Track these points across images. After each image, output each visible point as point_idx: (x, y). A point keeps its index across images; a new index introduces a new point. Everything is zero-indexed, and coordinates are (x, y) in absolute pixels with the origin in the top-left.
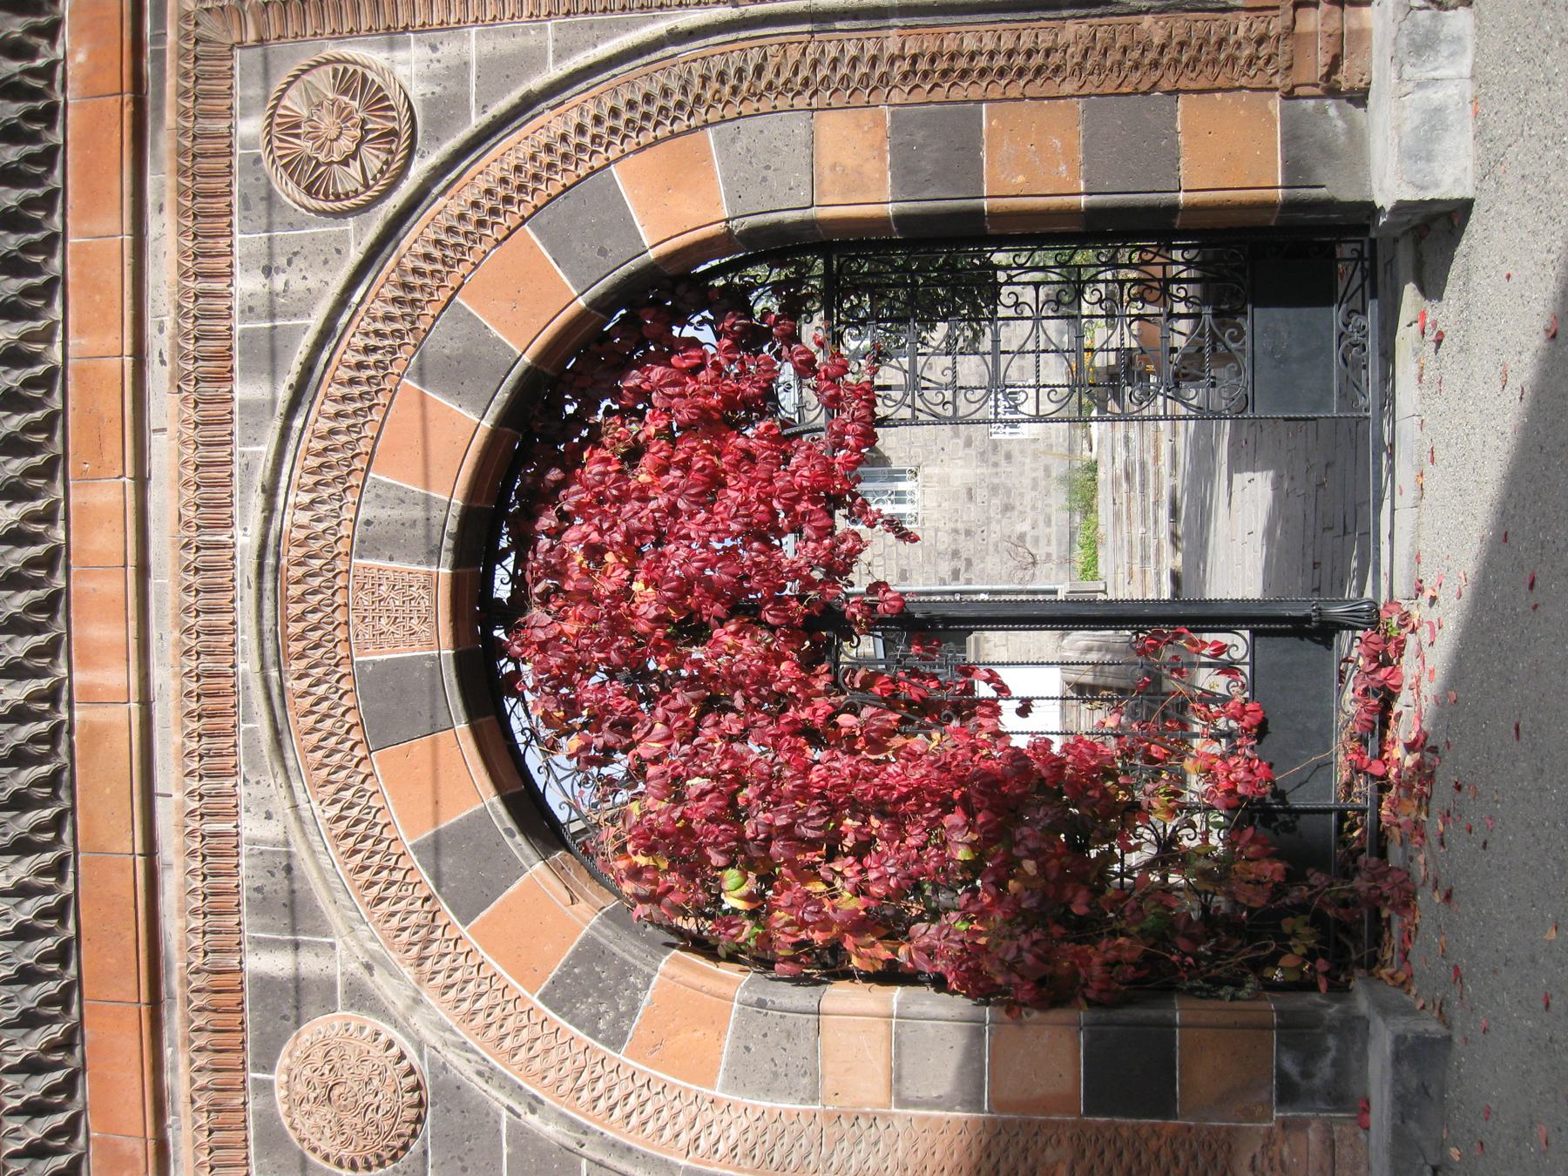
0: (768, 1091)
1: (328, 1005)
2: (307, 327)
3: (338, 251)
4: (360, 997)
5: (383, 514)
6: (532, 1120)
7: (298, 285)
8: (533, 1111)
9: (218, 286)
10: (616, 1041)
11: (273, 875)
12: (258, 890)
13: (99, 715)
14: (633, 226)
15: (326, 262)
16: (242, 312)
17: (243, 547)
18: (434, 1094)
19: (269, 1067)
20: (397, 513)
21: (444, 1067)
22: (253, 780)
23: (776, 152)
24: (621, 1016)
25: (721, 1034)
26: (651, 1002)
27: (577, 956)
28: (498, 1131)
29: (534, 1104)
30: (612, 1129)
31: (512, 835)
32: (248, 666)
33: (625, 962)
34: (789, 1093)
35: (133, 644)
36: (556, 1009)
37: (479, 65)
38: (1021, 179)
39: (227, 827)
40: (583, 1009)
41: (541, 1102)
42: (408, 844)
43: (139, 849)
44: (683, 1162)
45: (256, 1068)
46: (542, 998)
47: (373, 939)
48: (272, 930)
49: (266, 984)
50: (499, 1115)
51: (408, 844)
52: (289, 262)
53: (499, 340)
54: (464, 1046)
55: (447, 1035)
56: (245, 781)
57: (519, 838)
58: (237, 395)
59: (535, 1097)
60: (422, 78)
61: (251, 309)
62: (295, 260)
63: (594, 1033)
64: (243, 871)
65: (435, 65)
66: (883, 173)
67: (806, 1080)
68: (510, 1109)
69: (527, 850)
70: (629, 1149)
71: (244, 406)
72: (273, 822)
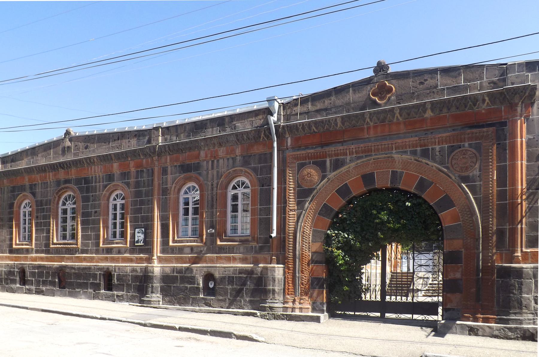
2: (429, 159)
5: (398, 174)
7: (437, 157)
9: (437, 143)
12: (339, 160)
13: (366, 130)
16: (433, 148)
17: (392, 153)
18: (310, 189)
22: (356, 157)
43: (345, 140)
47: (332, 178)
49: (325, 162)
52: (441, 155)
54: (317, 193)
61: (433, 149)
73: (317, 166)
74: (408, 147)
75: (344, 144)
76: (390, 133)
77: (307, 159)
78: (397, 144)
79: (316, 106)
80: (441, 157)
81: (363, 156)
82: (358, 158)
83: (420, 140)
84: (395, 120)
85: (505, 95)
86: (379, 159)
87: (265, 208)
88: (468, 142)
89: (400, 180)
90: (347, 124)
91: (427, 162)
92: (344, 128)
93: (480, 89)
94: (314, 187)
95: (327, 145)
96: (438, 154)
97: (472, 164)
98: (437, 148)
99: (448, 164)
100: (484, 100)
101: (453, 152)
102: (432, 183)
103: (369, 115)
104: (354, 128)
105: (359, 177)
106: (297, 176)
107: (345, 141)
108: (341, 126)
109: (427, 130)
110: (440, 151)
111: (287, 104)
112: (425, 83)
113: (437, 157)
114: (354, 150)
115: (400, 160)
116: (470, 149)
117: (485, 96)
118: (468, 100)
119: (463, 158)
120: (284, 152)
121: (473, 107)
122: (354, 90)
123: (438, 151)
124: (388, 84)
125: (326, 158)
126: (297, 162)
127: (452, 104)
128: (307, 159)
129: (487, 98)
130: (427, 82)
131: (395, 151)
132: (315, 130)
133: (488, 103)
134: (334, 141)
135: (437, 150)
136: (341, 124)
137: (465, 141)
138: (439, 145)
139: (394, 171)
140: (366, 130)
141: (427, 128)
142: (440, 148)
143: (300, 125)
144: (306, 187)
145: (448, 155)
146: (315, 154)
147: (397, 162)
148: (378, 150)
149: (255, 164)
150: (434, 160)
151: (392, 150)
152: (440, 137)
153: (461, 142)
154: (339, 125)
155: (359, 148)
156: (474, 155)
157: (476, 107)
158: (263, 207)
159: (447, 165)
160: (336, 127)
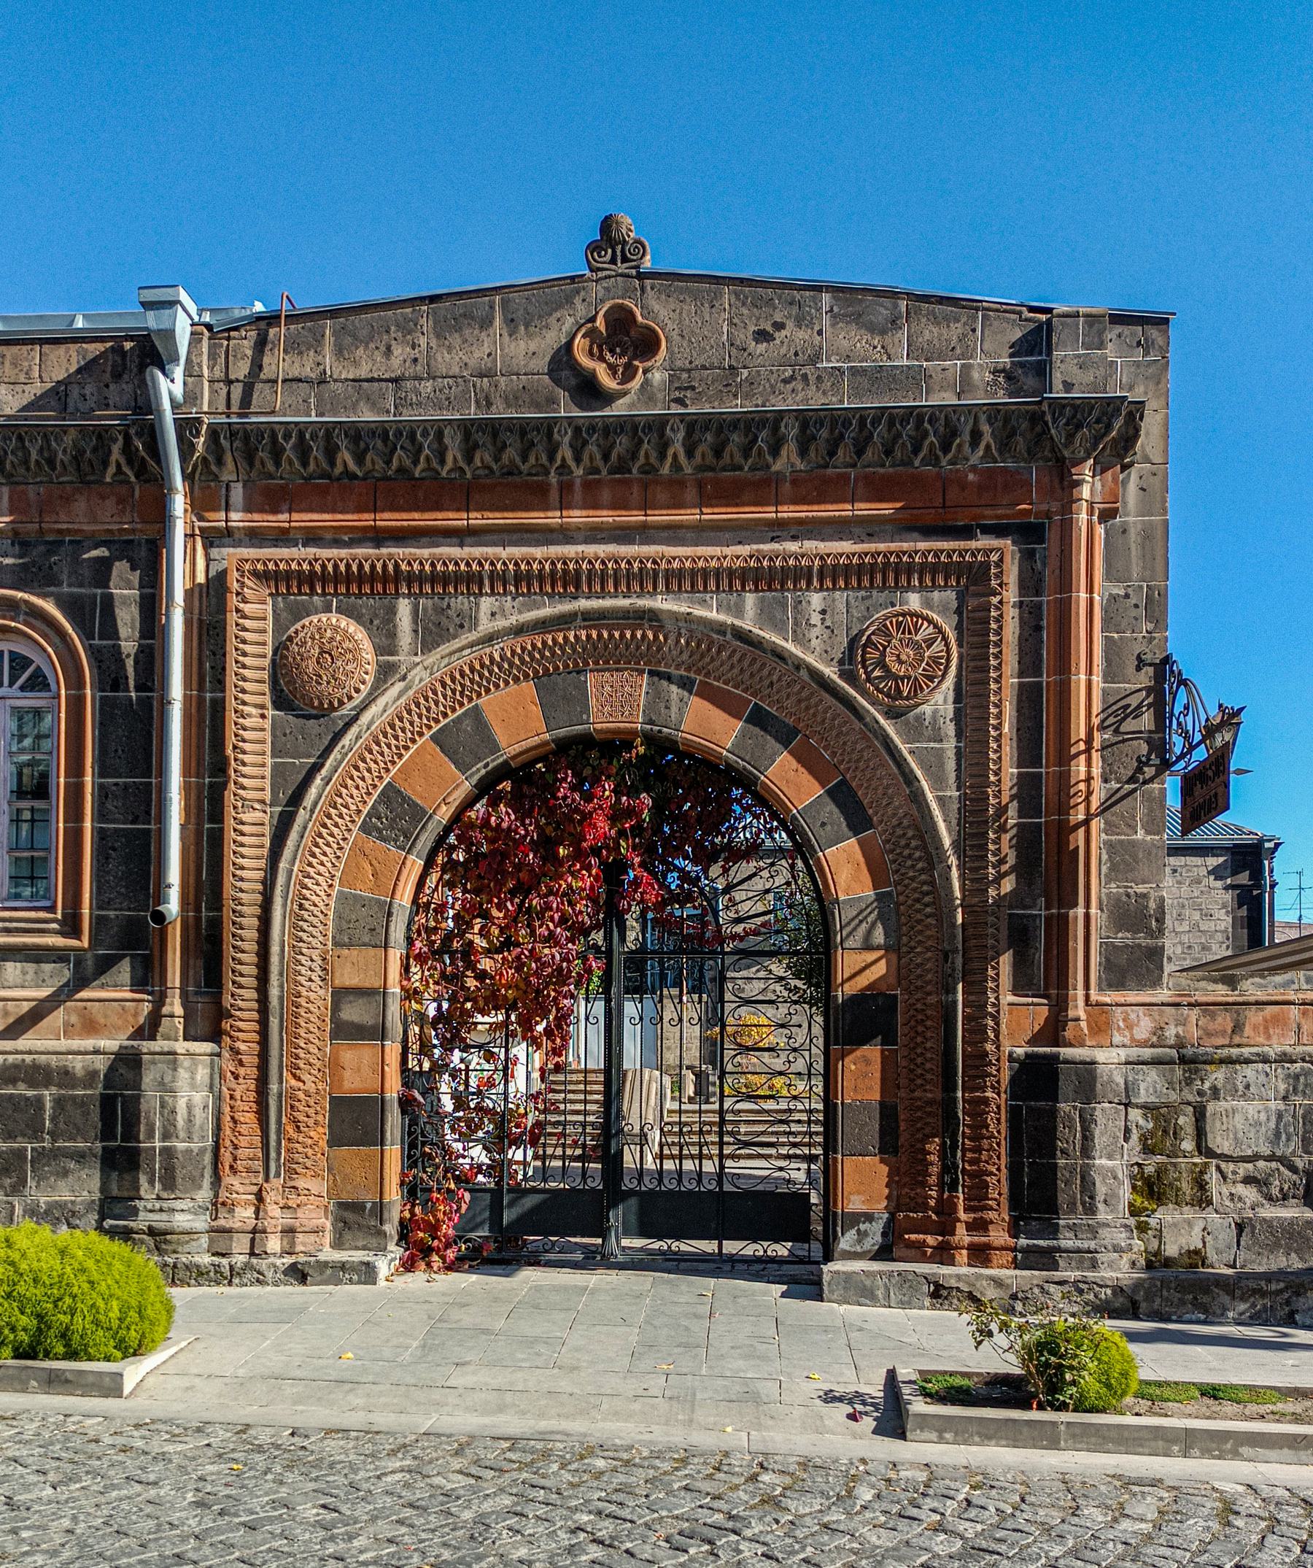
1: (379, 650)
7: (815, 632)
10: (365, 828)
15: (826, 652)
24: (379, 831)
32: (584, 604)
36: (383, 793)
40: (382, 809)
47: (421, 680)
52: (827, 627)
62: (828, 631)
75: (468, 540)
79: (356, 363)
84: (665, 470)
85: (1046, 423)
86: (604, 618)
87: (126, 786)
92: (469, 476)
93: (962, 391)
96: (815, 619)
100: (976, 436)
102: (797, 732)
104: (510, 478)
108: (461, 464)
110: (823, 612)
112: (777, 335)
117: (983, 418)
118: (926, 425)
121: (940, 453)
122: (512, 320)
124: (640, 319)
127: (871, 434)
129: (986, 428)
130: (784, 333)
132: (352, 466)
136: (459, 457)
149: (81, 585)
157: (950, 456)
158: (116, 784)
160: (435, 464)
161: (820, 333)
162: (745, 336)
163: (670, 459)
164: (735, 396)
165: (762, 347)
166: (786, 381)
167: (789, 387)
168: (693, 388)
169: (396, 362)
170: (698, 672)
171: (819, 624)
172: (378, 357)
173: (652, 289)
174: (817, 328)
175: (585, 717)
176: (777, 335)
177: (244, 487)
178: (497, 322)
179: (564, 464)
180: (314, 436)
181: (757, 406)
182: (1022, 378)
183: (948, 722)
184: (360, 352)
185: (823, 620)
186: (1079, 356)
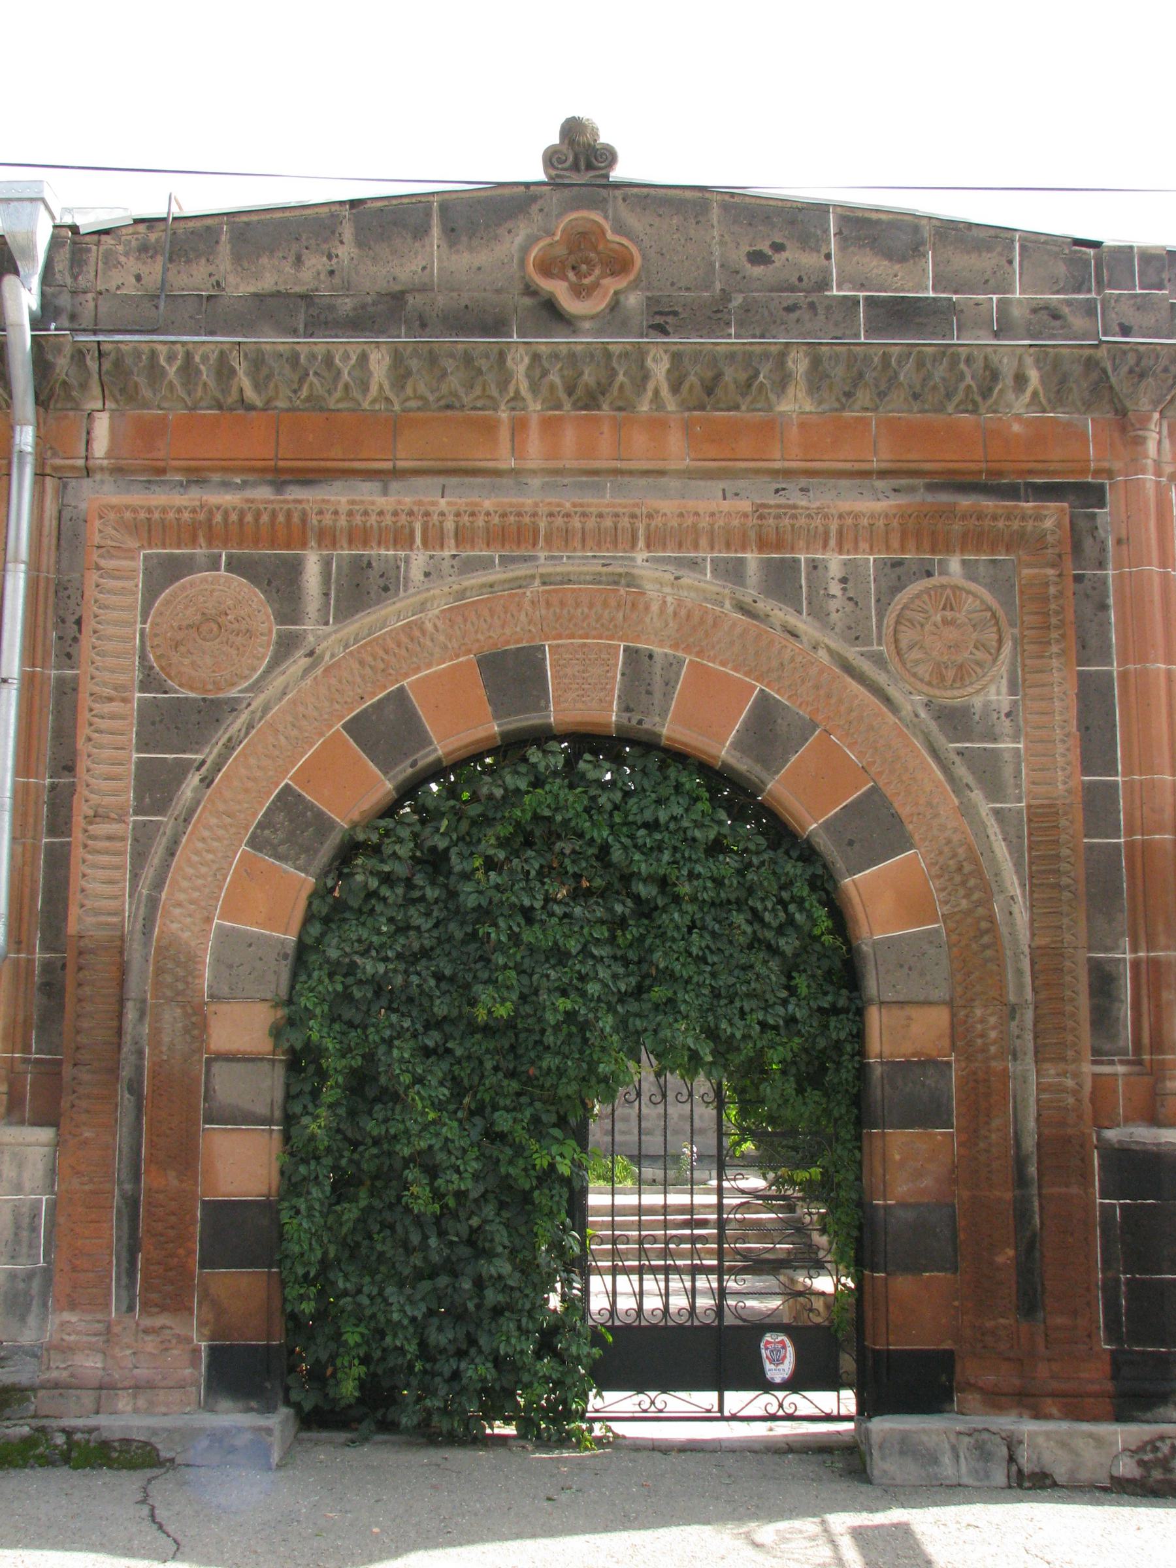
0: (218, 960)
1: (282, 618)
2: (800, 612)
3: (857, 638)
4: (287, 645)
5: (657, 669)
6: (194, 779)
7: (833, 605)
8: (202, 780)
9: (832, 542)
11: (382, 576)
12: (369, 565)
13: (504, 434)
14: (869, 867)
15: (850, 628)
16: (813, 560)
17: (633, 559)
18: (212, 701)
19: (230, 567)
20: (657, 679)
21: (233, 710)
22: (454, 562)
23: (922, 974)
24: (274, 848)
25: (258, 924)
26: (285, 871)
27: (320, 815)
28: (184, 752)
29: (207, 782)
30: (188, 841)
31: (412, 766)
33: (316, 852)
34: (216, 976)
35: (559, 464)
36: (279, 796)
37: (993, 750)
38: (897, 1157)
39: (418, 541)
40: (280, 817)
41: (208, 786)
42: (405, 683)
43: (401, 464)
44: (164, 895)
45: (230, 557)
46: (287, 785)
47: (333, 656)
48: (339, 574)
49: (295, 568)
50: (197, 752)
51: (405, 683)
52: (850, 599)
53: (787, 761)
54: (250, 726)
55: (259, 714)
56: (454, 556)
57: (410, 771)
58: (748, 555)
59: (212, 781)
60: (986, 705)
61: (815, 568)
62: (851, 604)
63: (260, 825)
64: (383, 552)
65: (995, 716)
66: (904, 1056)
67: (226, 989)
68: (203, 762)
69: (401, 777)
70: (173, 855)
71: (741, 561)
72: (422, 578)
73: (254, 579)
74: (703, 542)
75: (395, 485)
76: (619, 465)
77: (202, 540)
78: (658, 521)
80: (850, 607)
81: (492, 559)
82: (469, 566)
83: (761, 517)
84: (644, 407)
85: (1104, 371)
86: (569, 581)
88: (962, 552)
89: (668, 696)
90: (415, 390)
91: (792, 620)
92: (397, 407)
93: (1000, 330)
94: (233, 693)
95: (307, 478)
96: (835, 589)
97: (979, 655)
98: (834, 562)
99: (879, 644)
100: (1020, 380)
101: (896, 589)
102: (815, 726)
103: (527, 360)
104: (449, 413)
105: (468, 661)
106: (139, 626)
107: (397, 474)
108: (388, 392)
109: (788, 473)
110: (844, 580)
111: (95, 237)
112: (776, 257)
113: (833, 605)
114: (449, 525)
115: (669, 599)
116: (973, 586)
117: (1029, 361)
118: (962, 366)
119: (945, 622)
120: (65, 486)
121: (978, 399)
123: (839, 576)
125: (304, 545)
126: (142, 547)
127: (896, 374)
128: (202, 540)
129: (1034, 375)
131: (646, 555)
132: (250, 394)
133: (1035, 394)
134: (341, 465)
135: (831, 574)
136: (387, 386)
137: (949, 550)
138: (840, 553)
139: (637, 651)
140: (504, 434)
141: (787, 464)
142: (845, 563)
143: (171, 358)
144: (192, 689)
145: (878, 601)
146: (249, 518)
147: (655, 607)
148: (567, 536)
150: (819, 614)
151: (633, 546)
152: (849, 514)
153: (933, 551)
154: (374, 389)
155: (473, 514)
156: (989, 614)
157: (990, 401)
159: (875, 648)
160: (359, 397)
161: (828, 257)
162: (739, 256)
163: (650, 394)
164: (728, 324)
165: (758, 271)
166: (789, 309)
167: (794, 316)
168: (675, 314)
169: (307, 275)
170: (687, 649)
171: (838, 593)
172: (288, 269)
173: (624, 200)
174: (824, 251)
175: (543, 703)
176: (776, 257)
177: (111, 418)
178: (436, 231)
179: (517, 396)
180: (205, 358)
181: (754, 337)
182: (1071, 319)
183: (1003, 717)
184: (264, 260)
185: (844, 589)
186: (1135, 296)
